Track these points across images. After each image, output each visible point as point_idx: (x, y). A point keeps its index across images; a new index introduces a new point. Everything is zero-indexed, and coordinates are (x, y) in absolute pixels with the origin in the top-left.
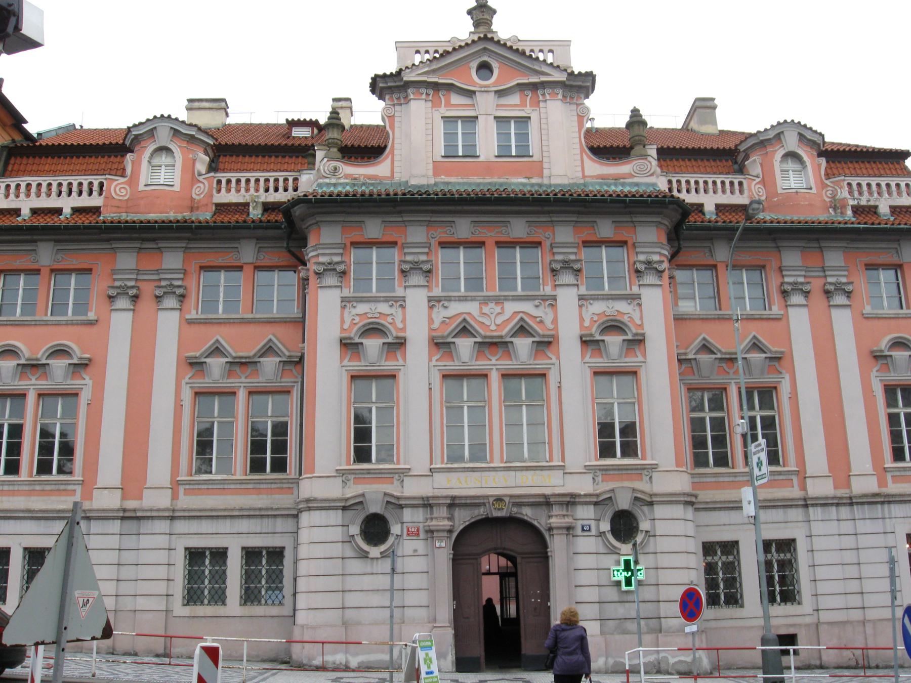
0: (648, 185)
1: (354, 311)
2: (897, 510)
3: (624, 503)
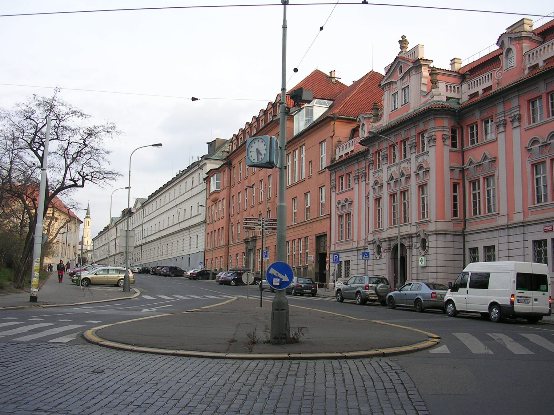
2: (530, 229)
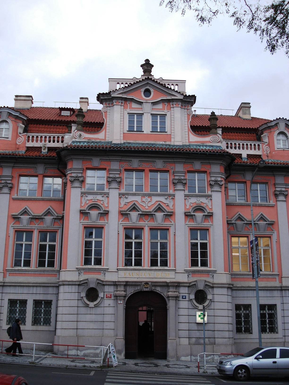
0: (217, 146)
1: (86, 198)
3: (201, 287)
